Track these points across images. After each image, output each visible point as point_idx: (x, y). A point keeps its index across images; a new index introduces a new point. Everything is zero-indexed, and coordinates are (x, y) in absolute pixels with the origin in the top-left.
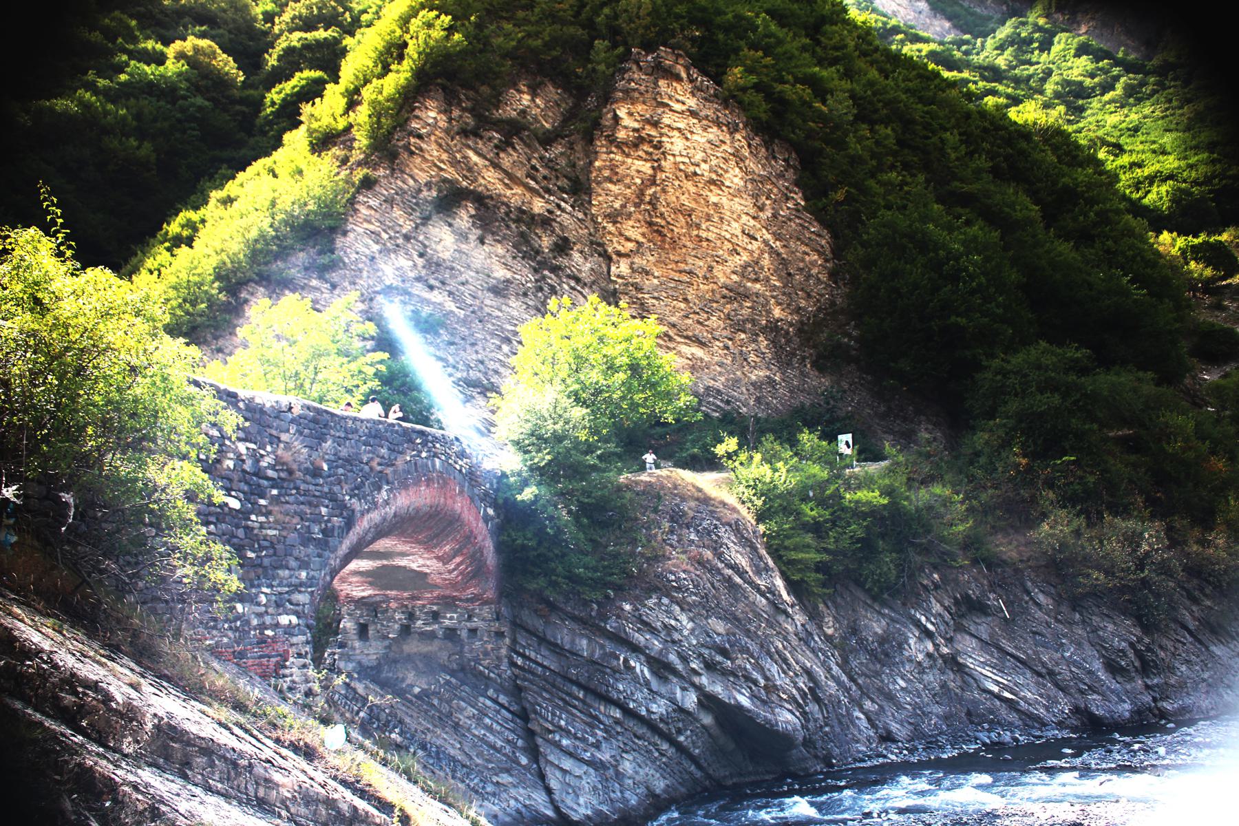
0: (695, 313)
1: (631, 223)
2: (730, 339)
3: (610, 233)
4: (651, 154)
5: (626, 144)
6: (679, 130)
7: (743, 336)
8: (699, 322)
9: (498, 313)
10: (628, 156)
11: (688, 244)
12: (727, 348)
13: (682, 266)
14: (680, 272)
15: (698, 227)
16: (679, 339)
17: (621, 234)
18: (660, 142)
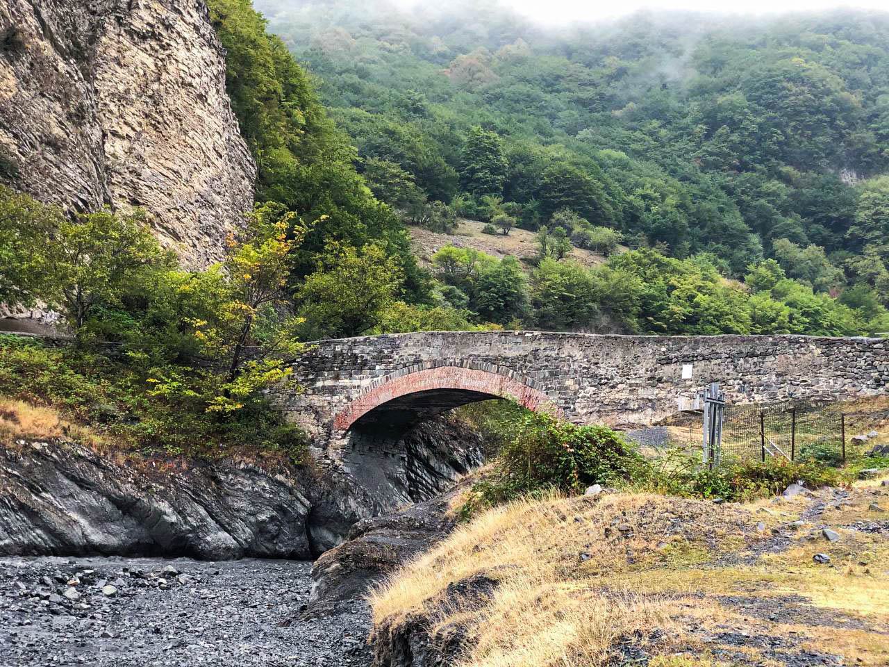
0: (175, 209)
1: (133, 110)
2: (198, 239)
3: (111, 112)
4: (156, 51)
5: (138, 34)
6: (185, 39)
7: (208, 239)
8: (178, 219)
9: (55, 170)
10: (135, 44)
11: (177, 145)
12: (195, 246)
13: (170, 164)
14: (168, 169)
15: (186, 132)
16: (158, 228)
17: (121, 116)
18: (169, 45)
